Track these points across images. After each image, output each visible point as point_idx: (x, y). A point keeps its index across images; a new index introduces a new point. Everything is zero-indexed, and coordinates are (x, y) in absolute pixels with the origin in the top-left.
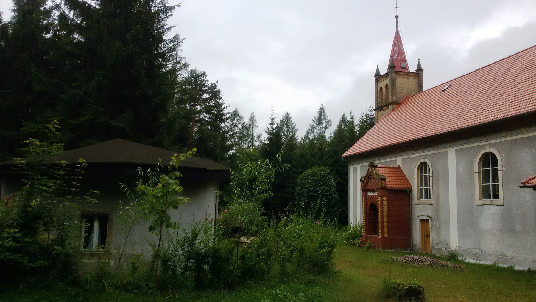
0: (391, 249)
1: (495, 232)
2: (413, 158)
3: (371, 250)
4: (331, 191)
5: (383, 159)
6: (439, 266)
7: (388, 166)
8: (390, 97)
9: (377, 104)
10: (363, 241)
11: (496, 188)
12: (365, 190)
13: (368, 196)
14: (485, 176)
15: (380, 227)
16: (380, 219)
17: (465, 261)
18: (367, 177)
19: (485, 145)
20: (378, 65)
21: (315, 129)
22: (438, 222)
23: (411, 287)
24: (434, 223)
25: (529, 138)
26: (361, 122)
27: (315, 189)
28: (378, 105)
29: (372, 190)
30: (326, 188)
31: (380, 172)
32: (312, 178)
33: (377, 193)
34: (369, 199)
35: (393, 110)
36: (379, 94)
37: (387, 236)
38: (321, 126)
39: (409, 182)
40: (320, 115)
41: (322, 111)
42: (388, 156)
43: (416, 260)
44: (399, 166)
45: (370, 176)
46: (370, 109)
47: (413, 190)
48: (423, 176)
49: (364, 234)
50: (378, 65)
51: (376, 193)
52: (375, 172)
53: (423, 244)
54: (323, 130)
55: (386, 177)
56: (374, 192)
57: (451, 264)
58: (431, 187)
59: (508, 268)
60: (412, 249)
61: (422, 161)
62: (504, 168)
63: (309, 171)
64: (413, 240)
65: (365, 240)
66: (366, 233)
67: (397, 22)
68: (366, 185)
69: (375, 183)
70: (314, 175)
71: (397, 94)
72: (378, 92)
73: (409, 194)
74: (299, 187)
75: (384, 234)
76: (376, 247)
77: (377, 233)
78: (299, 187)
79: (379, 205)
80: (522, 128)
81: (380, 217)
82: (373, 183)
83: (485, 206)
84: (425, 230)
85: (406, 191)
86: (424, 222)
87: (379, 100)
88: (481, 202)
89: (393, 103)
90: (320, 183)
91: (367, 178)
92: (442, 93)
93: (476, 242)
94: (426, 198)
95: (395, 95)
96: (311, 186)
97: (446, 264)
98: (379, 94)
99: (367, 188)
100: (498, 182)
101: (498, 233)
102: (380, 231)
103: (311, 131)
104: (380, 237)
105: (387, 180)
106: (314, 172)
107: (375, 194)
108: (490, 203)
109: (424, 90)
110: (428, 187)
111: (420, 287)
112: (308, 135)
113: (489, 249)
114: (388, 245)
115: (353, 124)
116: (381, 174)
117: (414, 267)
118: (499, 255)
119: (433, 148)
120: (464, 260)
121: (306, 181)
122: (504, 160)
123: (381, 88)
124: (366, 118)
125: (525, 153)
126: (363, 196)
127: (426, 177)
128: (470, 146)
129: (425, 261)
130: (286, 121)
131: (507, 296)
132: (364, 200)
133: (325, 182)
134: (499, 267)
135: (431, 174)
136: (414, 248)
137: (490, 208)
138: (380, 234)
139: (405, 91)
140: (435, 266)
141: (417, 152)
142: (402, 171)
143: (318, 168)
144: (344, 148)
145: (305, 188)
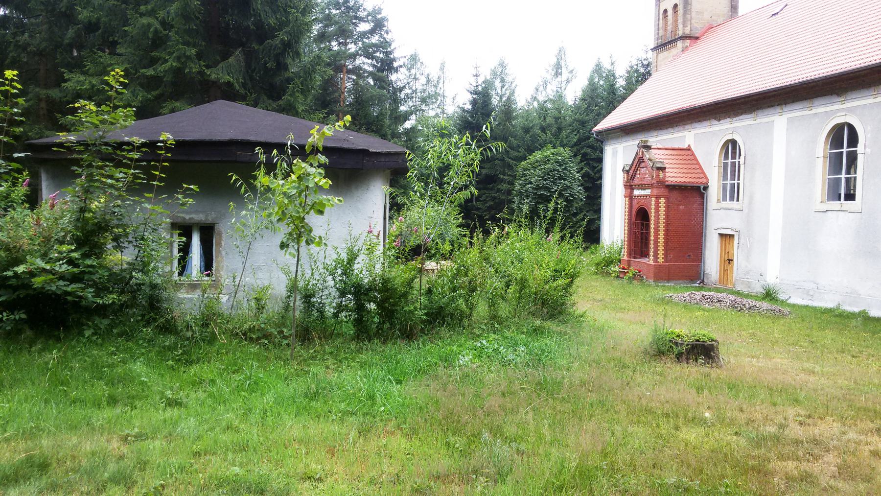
0: (669, 280)
3: (635, 282)
4: (573, 189)
6: (745, 309)
7: (669, 147)
8: (680, 26)
10: (624, 268)
11: (851, 183)
12: (629, 186)
14: (835, 164)
15: (652, 246)
16: (652, 234)
17: (788, 302)
18: (635, 164)
19: (839, 110)
21: (548, 83)
23: (698, 341)
24: (742, 241)
26: (628, 72)
27: (547, 184)
29: (642, 187)
30: (564, 184)
31: (656, 156)
32: (542, 167)
33: (650, 191)
34: (635, 202)
35: (684, 50)
36: (661, 21)
37: (663, 260)
38: (559, 79)
39: (704, 173)
40: (558, 59)
41: (561, 53)
42: (670, 130)
43: (709, 300)
44: (689, 146)
46: (645, 49)
47: (709, 188)
48: (729, 164)
49: (626, 258)
51: (648, 192)
52: (647, 156)
54: (562, 85)
55: (666, 166)
56: (645, 189)
57: (765, 305)
58: (741, 182)
59: (860, 312)
60: (703, 282)
61: (730, 137)
62: (868, 150)
63: (538, 155)
64: (706, 268)
65: (626, 267)
66: (629, 255)
69: (647, 176)
70: (545, 162)
71: (693, 21)
72: (659, 19)
73: (704, 194)
74: (521, 182)
75: (659, 258)
76: (644, 277)
77: (645, 255)
78: (521, 182)
79: (653, 211)
81: (652, 230)
82: (645, 174)
84: (727, 251)
85: (700, 187)
86: (726, 238)
87: (660, 31)
88: (824, 207)
89: (684, 37)
90: (555, 176)
91: (634, 167)
92: (771, 19)
93: (809, 272)
94: (732, 199)
95: (689, 22)
96: (540, 180)
97: (757, 306)
98: (661, 21)
99: (632, 184)
102: (651, 254)
103: (541, 88)
104: (651, 262)
105: (667, 170)
106: (546, 157)
109: (740, 14)
110: (736, 182)
111: (713, 340)
112: (536, 94)
114: (663, 275)
115: (614, 75)
116: (657, 160)
117: (704, 310)
119: (750, 116)
120: (787, 300)
121: (532, 171)
122: (869, 135)
123: (666, 11)
124: (637, 65)
126: (625, 196)
127: (733, 164)
128: (814, 111)
129: (723, 300)
130: (500, 70)
131: (853, 357)
132: (627, 203)
133: (564, 173)
134: (844, 311)
135: (742, 160)
136: (705, 280)
138: (651, 258)
139: (706, 16)
140: (739, 309)
142: (693, 154)
143: (553, 151)
144: (596, 117)
145: (531, 183)
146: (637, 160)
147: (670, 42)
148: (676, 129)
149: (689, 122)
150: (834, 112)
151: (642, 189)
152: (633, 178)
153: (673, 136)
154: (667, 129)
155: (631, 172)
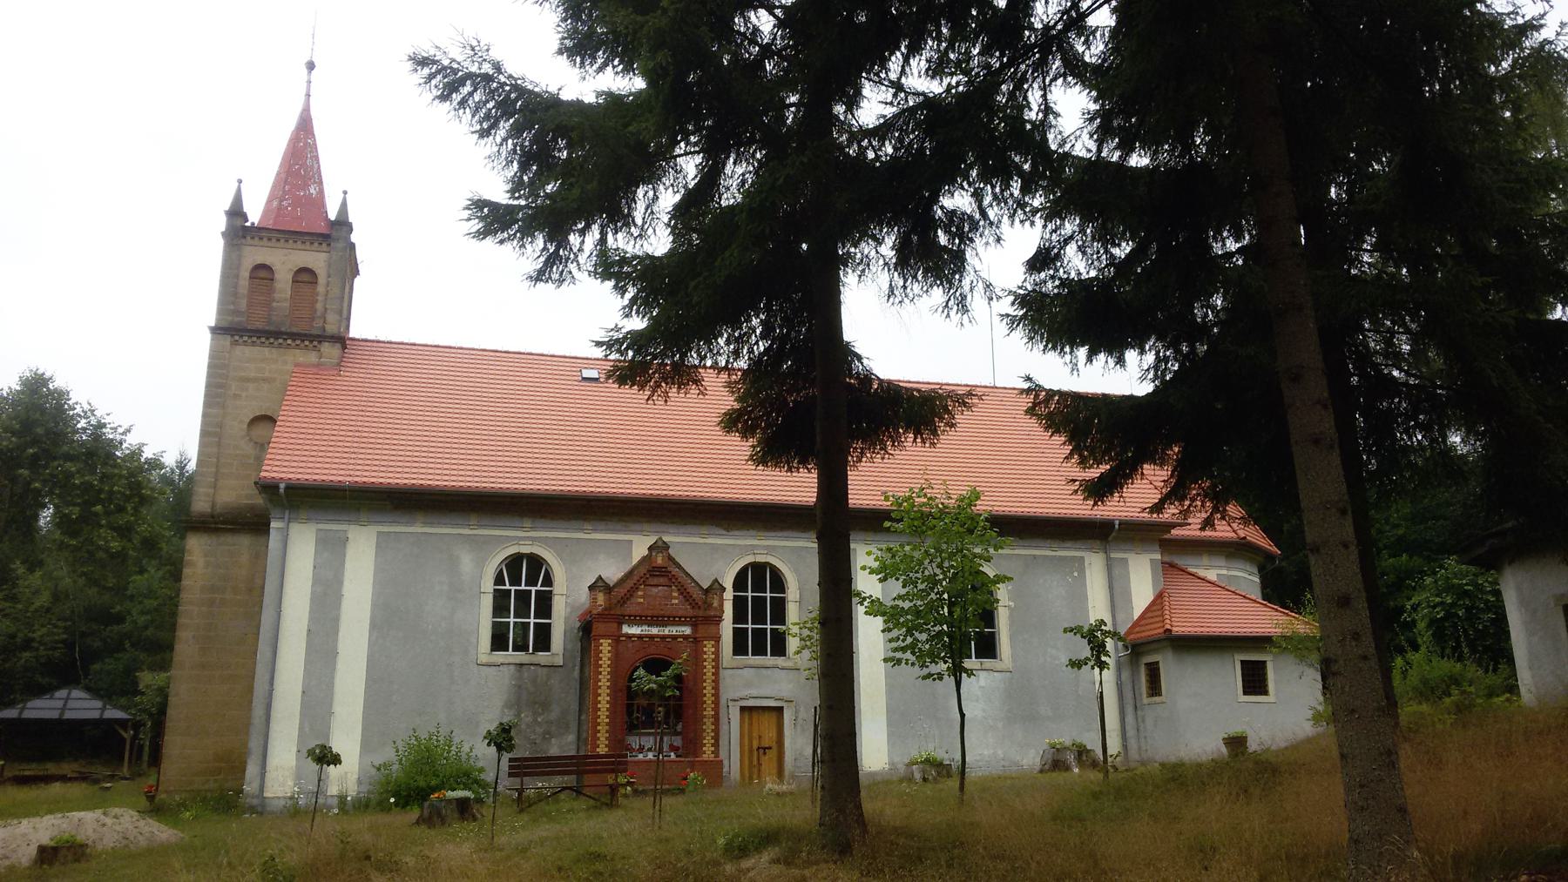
2: (715, 548)
9: (222, 310)
13: (629, 637)
18: (636, 578)
20: (240, 181)
28: (236, 319)
45: (648, 576)
50: (240, 181)
53: (747, 773)
67: (309, 82)
68: (619, 602)
80: (1047, 538)
94: (759, 650)
101: (1000, 725)
107: (674, 633)
113: (978, 758)
118: (1004, 766)
125: (1055, 583)
141: (736, 533)
146: (643, 570)
147: (294, 336)
152: (624, 601)
154: (570, 519)
155: (622, 591)
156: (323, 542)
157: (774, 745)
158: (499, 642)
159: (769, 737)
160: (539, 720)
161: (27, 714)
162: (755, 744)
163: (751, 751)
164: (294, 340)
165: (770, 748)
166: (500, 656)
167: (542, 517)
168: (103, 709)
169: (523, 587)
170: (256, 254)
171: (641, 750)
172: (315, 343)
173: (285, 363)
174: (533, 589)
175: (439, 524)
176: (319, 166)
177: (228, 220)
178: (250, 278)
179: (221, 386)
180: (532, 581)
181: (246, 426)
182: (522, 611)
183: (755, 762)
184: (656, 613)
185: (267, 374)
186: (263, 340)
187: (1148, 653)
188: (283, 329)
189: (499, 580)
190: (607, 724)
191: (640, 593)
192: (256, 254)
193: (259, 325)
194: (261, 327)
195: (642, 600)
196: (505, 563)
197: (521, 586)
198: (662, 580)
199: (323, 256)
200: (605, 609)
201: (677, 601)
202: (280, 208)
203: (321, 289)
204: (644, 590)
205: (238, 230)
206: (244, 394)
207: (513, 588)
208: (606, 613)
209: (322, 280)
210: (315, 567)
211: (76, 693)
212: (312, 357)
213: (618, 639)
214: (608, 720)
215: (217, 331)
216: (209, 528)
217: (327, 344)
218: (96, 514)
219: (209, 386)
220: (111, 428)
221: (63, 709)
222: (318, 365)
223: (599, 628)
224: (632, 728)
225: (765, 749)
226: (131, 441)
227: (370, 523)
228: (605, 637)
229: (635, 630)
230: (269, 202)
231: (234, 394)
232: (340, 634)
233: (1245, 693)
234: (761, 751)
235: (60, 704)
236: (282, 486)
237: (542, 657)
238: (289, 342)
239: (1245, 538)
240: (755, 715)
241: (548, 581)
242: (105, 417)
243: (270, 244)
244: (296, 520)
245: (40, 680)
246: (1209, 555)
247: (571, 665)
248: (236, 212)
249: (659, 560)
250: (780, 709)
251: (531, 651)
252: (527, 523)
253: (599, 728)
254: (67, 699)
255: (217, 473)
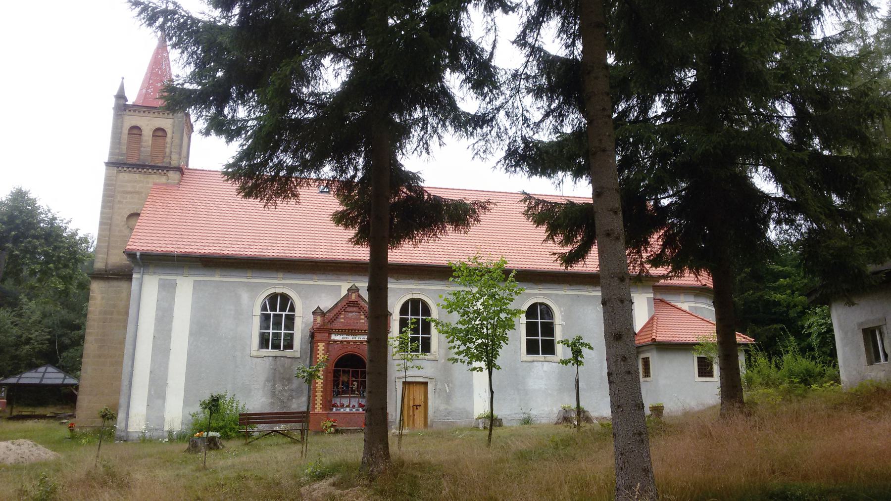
1: (550, 392)
5: (295, 279)
13: (335, 341)
19: (536, 294)
20: (123, 78)
22: (448, 385)
24: (438, 387)
25: (594, 296)
28: (120, 158)
50: (123, 78)
83: (535, 363)
100: (553, 337)
107: (362, 339)
108: (543, 359)
125: (590, 311)
137: (543, 365)
141: (402, 281)
147: (153, 167)
148: (324, 277)
149: (348, 273)
150: (529, 296)
151: (347, 335)
152: (332, 321)
153: (315, 283)
154: (305, 273)
155: (332, 315)
156: (163, 286)
157: (422, 404)
158: (264, 342)
159: (419, 399)
160: (286, 388)
161: (22, 381)
162: (411, 405)
163: (409, 407)
164: (153, 170)
165: (420, 406)
166: (264, 352)
167: (289, 272)
168: (64, 378)
169: (278, 312)
170: (132, 120)
171: (342, 406)
172: (165, 171)
173: (148, 182)
174: (284, 313)
175: (231, 276)
176: (170, 70)
177: (116, 101)
178: (129, 134)
179: (112, 196)
180: (283, 309)
181: (125, 219)
182: (277, 325)
183: (411, 414)
184: (350, 328)
185: (137, 190)
186: (135, 169)
187: (643, 352)
188: (147, 163)
189: (264, 308)
190: (322, 392)
191: (342, 316)
192: (132, 120)
193: (134, 161)
194: (134, 162)
195: (343, 320)
196: (268, 298)
197: (276, 311)
198: (355, 309)
199: (170, 121)
200: (320, 326)
201: (363, 321)
202: (147, 94)
203: (168, 140)
204: (344, 315)
205: (122, 107)
206: (125, 201)
207: (272, 313)
208: (322, 327)
209: (169, 135)
210: (158, 301)
211: (50, 369)
212: (163, 180)
213: (328, 343)
214: (322, 389)
215: (109, 164)
216: (104, 278)
217: (172, 172)
218: (50, 269)
219: (104, 196)
220: (60, 220)
221: (43, 377)
222: (166, 184)
223: (318, 336)
224: (338, 393)
225: (417, 406)
226: (71, 228)
227: (189, 275)
228: (321, 341)
229: (339, 338)
230: (141, 90)
231: (119, 201)
232: (172, 339)
233: (699, 376)
234: (415, 407)
235: (40, 375)
236: (138, 254)
237: (288, 352)
238: (150, 170)
239: (706, 285)
240: (411, 386)
241: (292, 309)
242: (57, 213)
243: (139, 115)
244: (148, 273)
245: (35, 361)
246: (685, 294)
247: (304, 357)
248: (121, 96)
249: (353, 297)
250: (426, 384)
251: (282, 349)
252: (280, 275)
253: (316, 394)
254: (45, 373)
255: (108, 246)
